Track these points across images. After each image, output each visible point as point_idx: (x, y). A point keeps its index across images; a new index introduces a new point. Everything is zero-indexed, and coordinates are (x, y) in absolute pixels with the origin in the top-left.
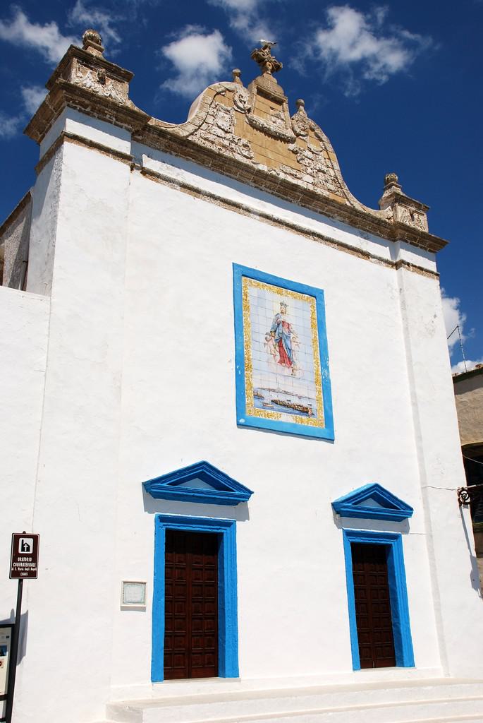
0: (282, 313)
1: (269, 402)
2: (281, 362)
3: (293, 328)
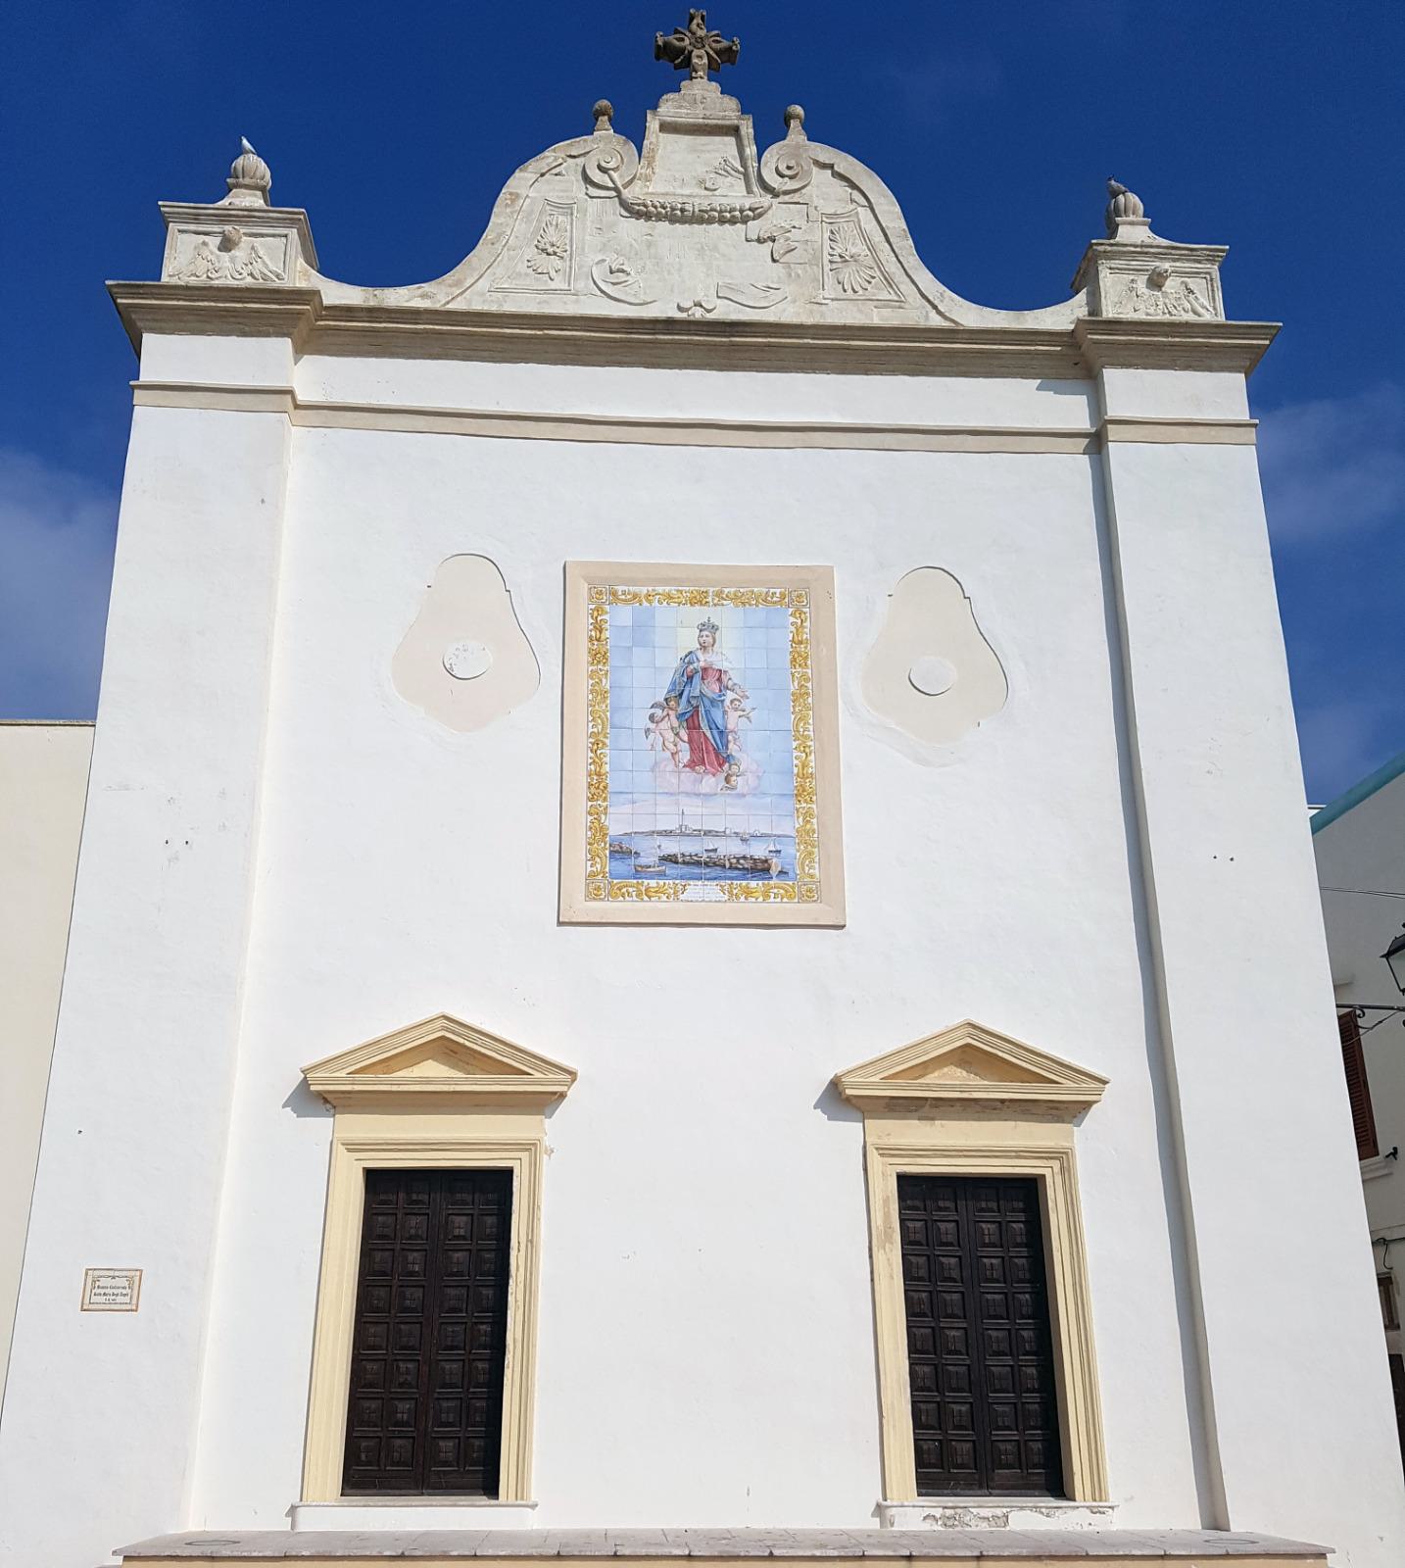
0: (703, 647)
1: (653, 860)
2: (692, 765)
3: (734, 677)
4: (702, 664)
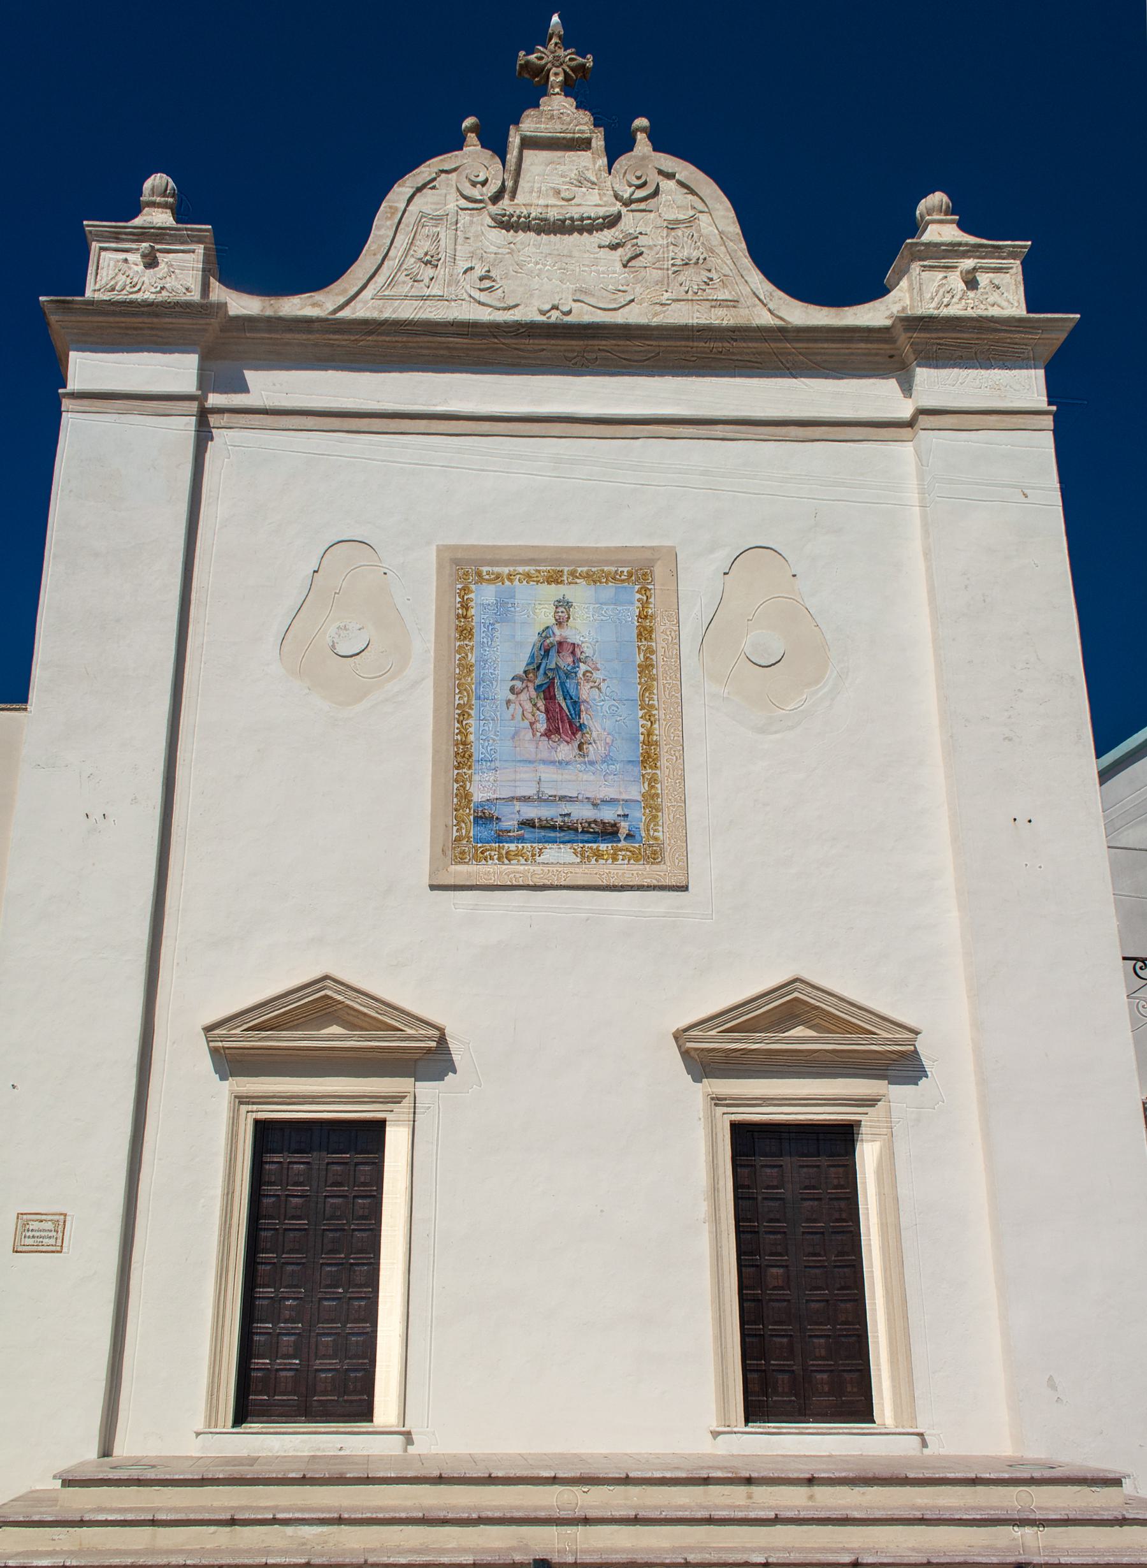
0: (559, 623)
2: (548, 734)
4: (558, 639)
